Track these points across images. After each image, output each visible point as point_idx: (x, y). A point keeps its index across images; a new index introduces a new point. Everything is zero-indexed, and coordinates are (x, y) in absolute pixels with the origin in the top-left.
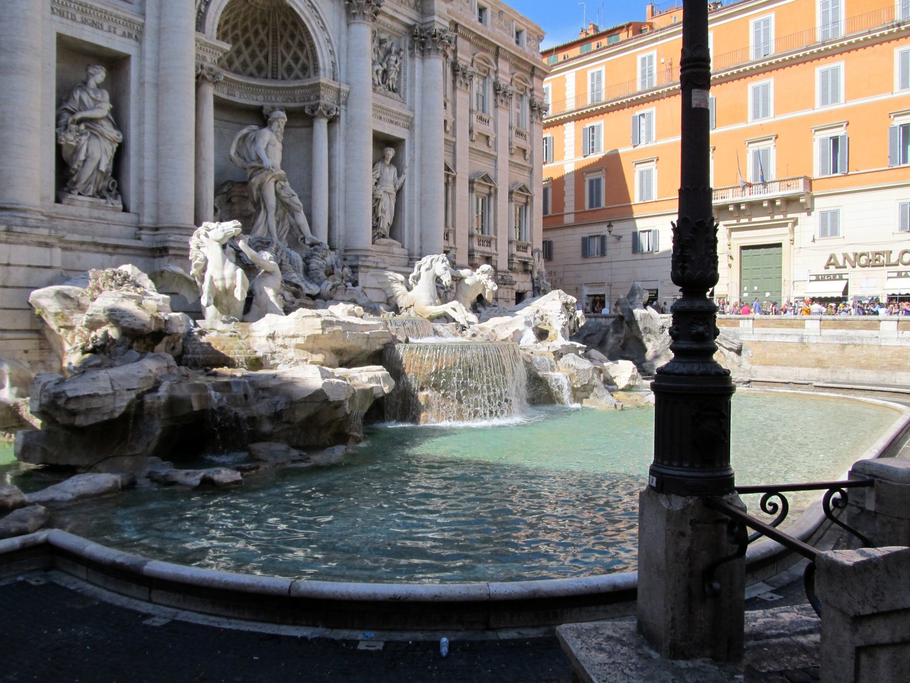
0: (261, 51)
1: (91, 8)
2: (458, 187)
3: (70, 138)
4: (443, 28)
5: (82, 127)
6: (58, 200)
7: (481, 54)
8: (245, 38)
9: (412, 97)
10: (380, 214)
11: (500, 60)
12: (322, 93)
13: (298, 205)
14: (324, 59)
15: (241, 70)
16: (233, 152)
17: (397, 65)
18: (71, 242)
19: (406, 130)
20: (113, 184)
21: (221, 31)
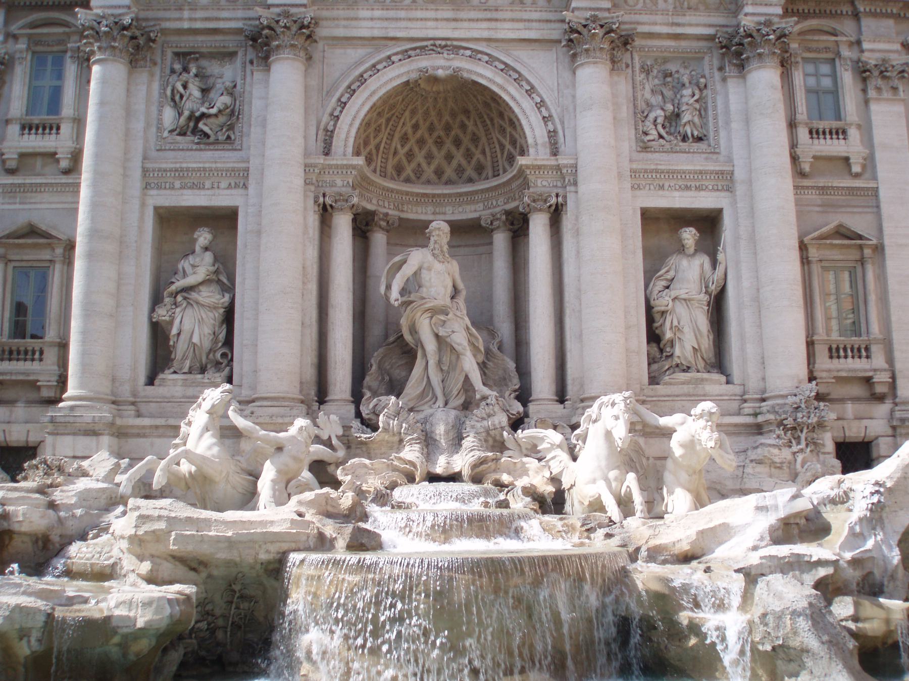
0: (477, 146)
1: (188, 169)
3: (162, 313)
4: (762, 19)
6: (151, 381)
8: (450, 139)
9: (729, 140)
10: (668, 335)
12: (531, 178)
13: (458, 344)
14: (534, 129)
15: (454, 176)
16: (382, 289)
17: (692, 101)
18: (144, 427)
19: (723, 194)
20: (224, 355)
21: (412, 142)
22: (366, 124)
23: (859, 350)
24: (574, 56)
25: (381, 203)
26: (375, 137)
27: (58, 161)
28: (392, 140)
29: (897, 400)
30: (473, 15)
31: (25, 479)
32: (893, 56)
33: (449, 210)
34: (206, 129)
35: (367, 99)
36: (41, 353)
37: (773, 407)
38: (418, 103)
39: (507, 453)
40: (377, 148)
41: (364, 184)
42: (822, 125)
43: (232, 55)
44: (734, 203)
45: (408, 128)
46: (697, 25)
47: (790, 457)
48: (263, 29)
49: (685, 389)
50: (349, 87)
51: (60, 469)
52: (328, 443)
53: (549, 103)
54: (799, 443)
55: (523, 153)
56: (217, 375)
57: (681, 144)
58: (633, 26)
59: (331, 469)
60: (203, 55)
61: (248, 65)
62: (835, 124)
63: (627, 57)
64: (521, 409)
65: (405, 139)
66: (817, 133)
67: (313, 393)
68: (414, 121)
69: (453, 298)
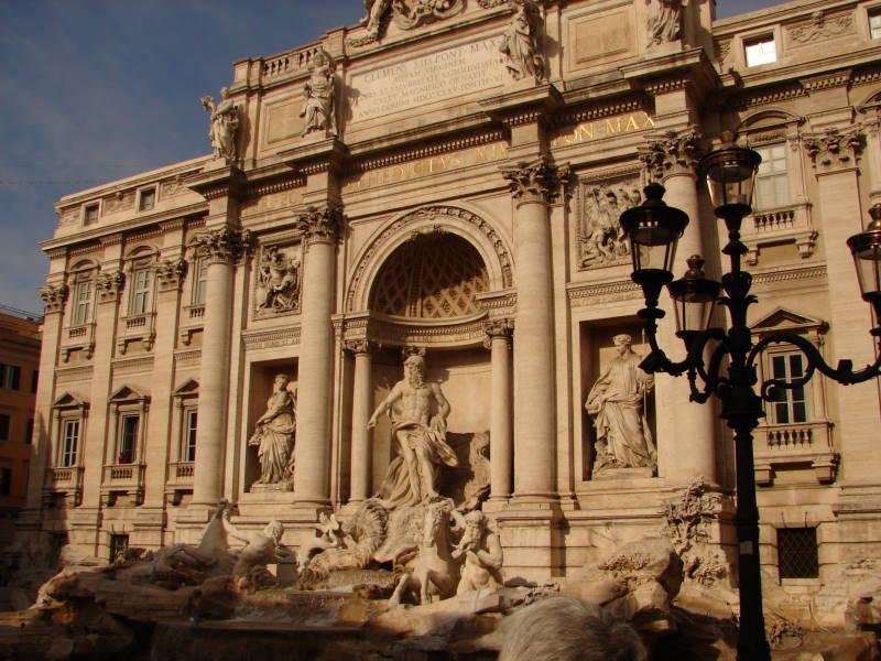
1: (268, 333)
6: (247, 490)
10: (599, 435)
25: (410, 338)
26: (401, 287)
28: (418, 286)
34: (280, 301)
35: (378, 261)
37: (664, 500)
40: (405, 294)
43: (299, 242)
49: (614, 483)
53: (504, 242)
57: (617, 257)
58: (564, 162)
66: (765, 220)
67: (334, 495)
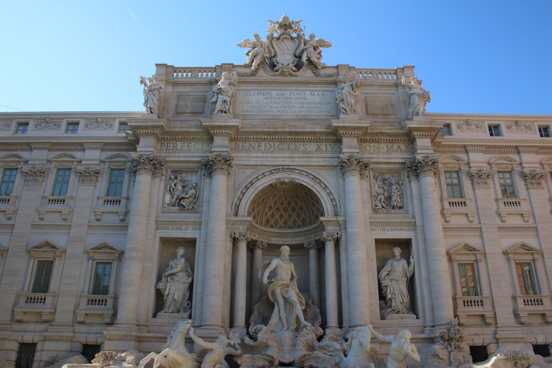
2: (489, 261)
3: (161, 285)
4: (425, 155)
5: (169, 278)
6: (154, 316)
7: (498, 156)
8: (291, 207)
9: (413, 208)
10: (389, 296)
11: (522, 154)
13: (295, 302)
16: (260, 276)
17: (396, 191)
19: (411, 232)
20: (188, 304)
21: (274, 208)
22: (253, 202)
23: (478, 302)
24: (344, 173)
25: (260, 237)
27: (119, 215)
29: (498, 326)
30: (300, 155)
31: (95, 362)
32: (484, 169)
33: (289, 239)
34: (184, 204)
35: (254, 191)
36: (106, 301)
38: (276, 193)
39: (316, 352)
41: (252, 228)
42: (454, 200)
43: (197, 172)
44: (416, 236)
45: (272, 203)
46: (397, 158)
47: (448, 354)
48: (210, 161)
50: (246, 186)
51: (112, 358)
52: (234, 347)
53: (333, 193)
54: (451, 347)
55: (323, 214)
56: (184, 314)
59: (235, 359)
60: (184, 172)
61: (203, 177)
62: (460, 200)
63: (367, 173)
64: (322, 331)
65: (270, 208)
66: (453, 203)
68: (274, 201)
69: (291, 280)
